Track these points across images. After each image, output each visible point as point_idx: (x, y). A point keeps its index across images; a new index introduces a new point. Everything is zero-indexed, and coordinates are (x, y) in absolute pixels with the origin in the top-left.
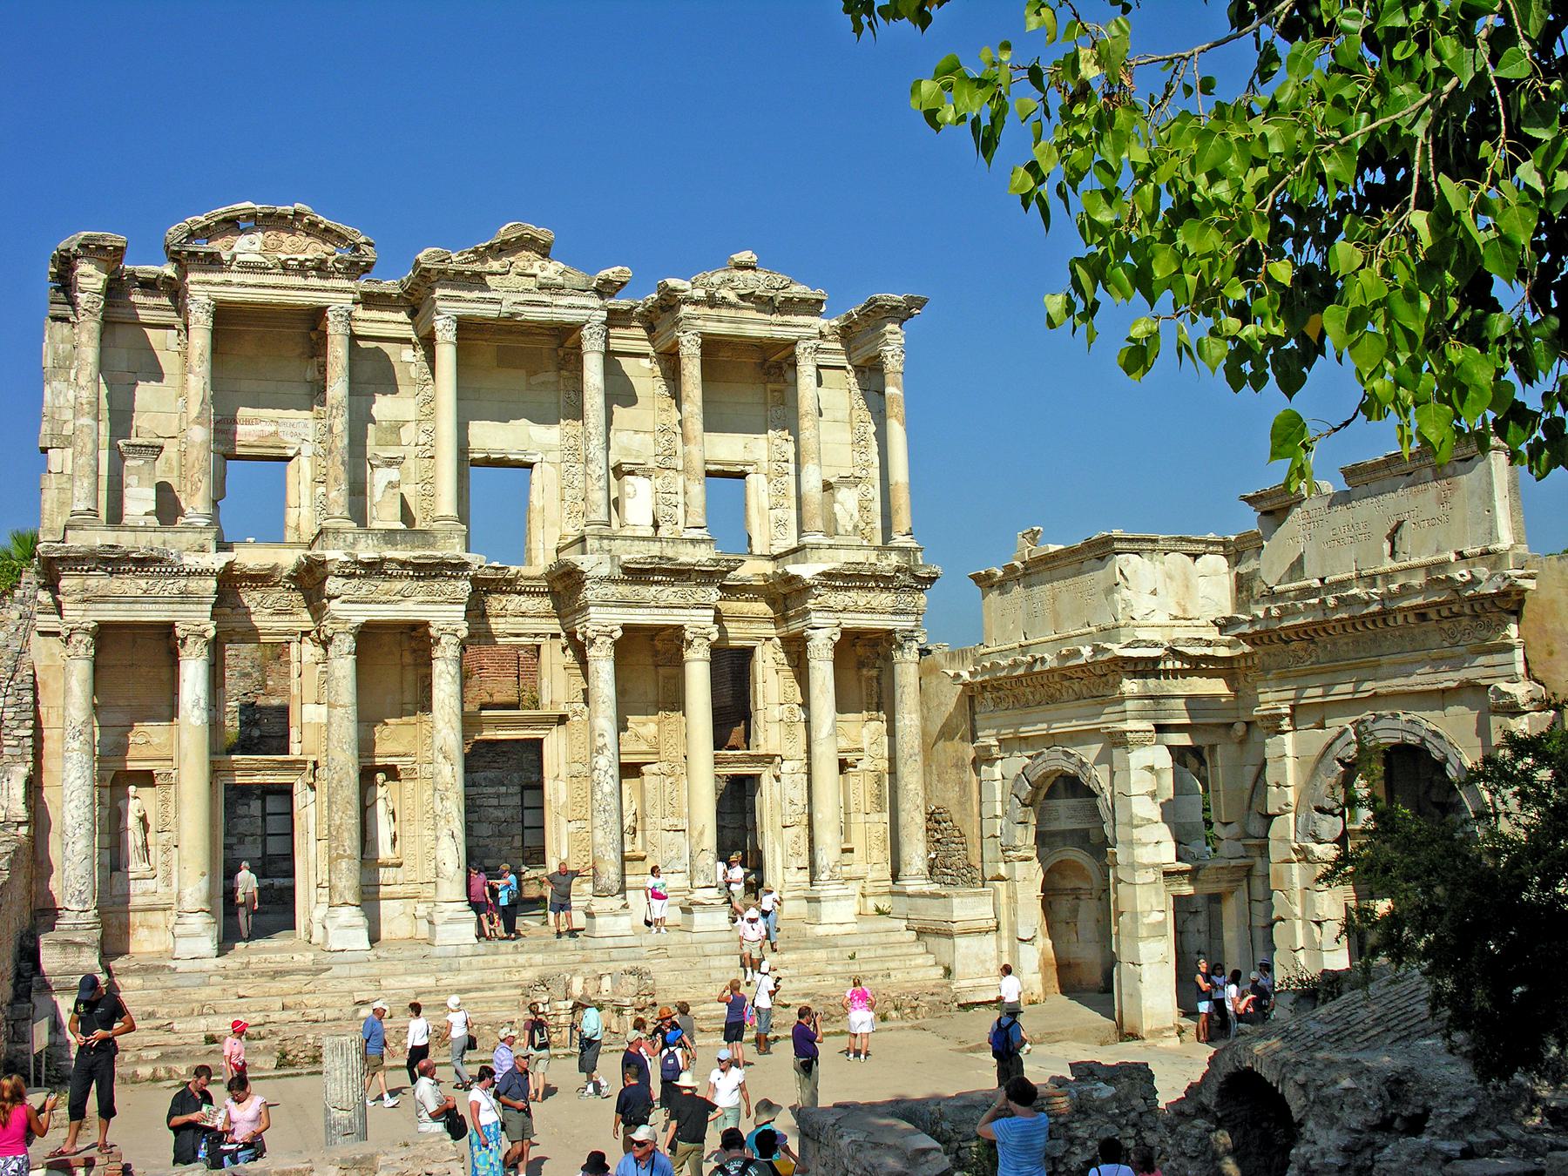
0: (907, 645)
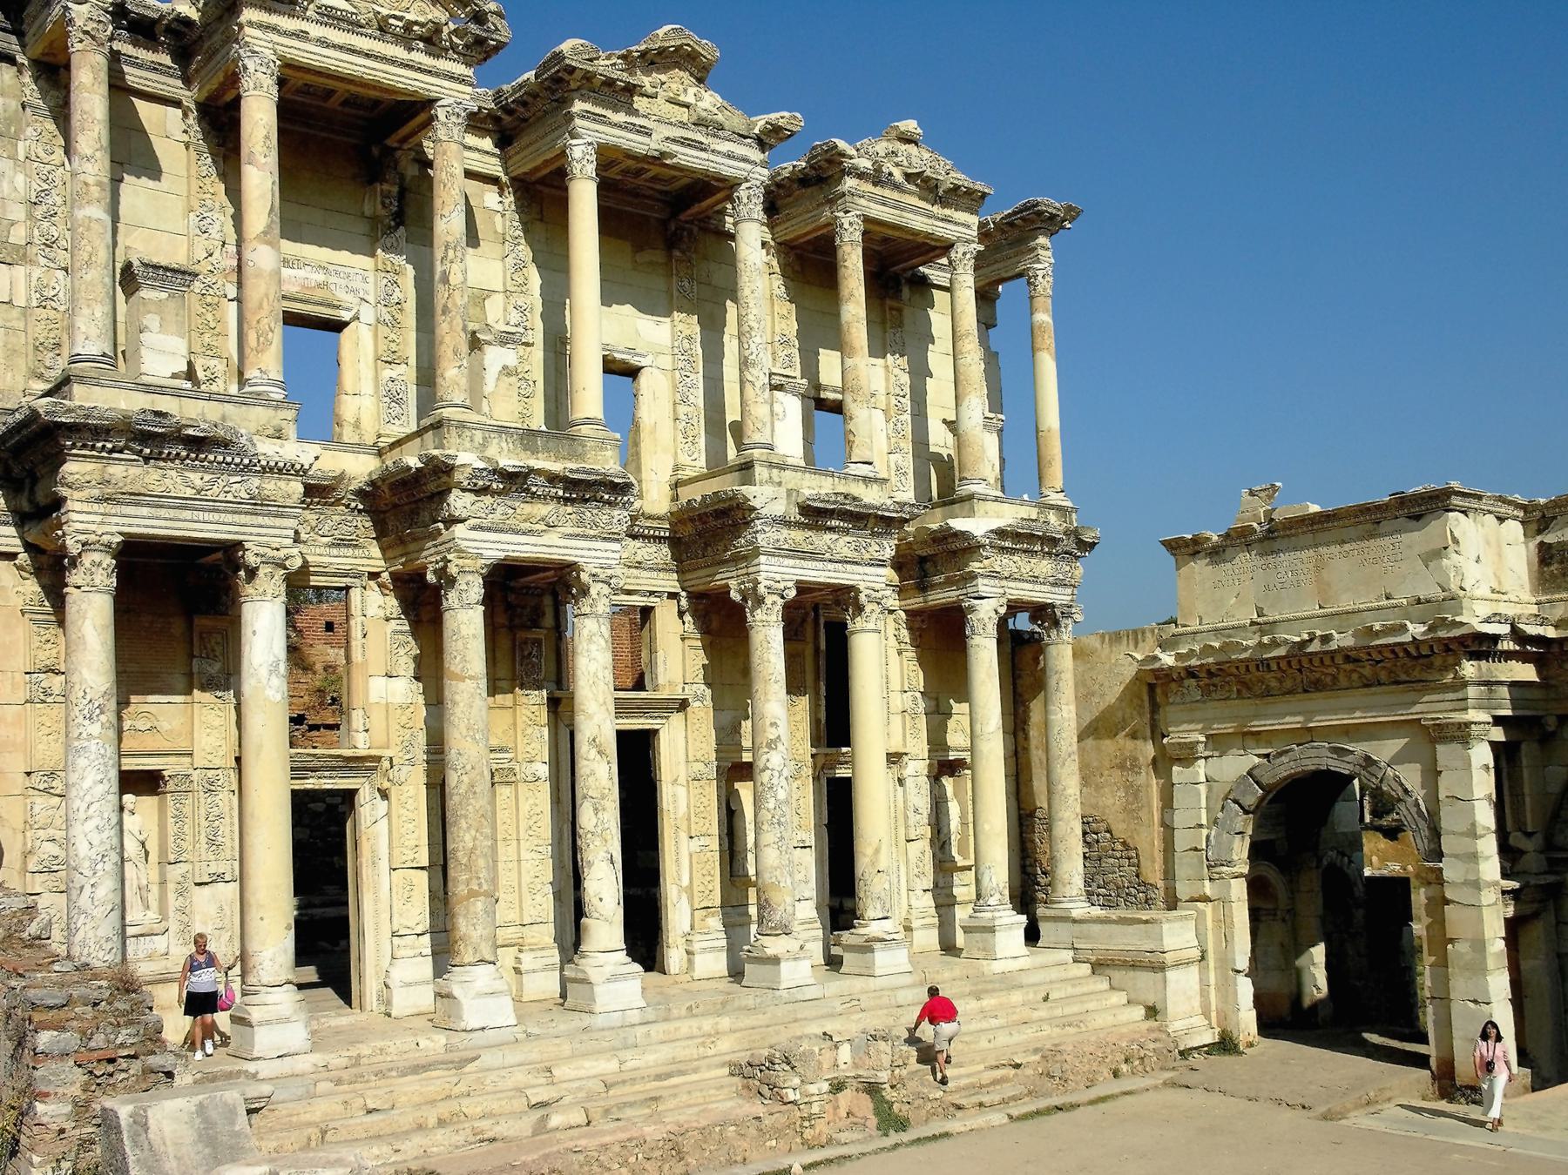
0: (1063, 622)
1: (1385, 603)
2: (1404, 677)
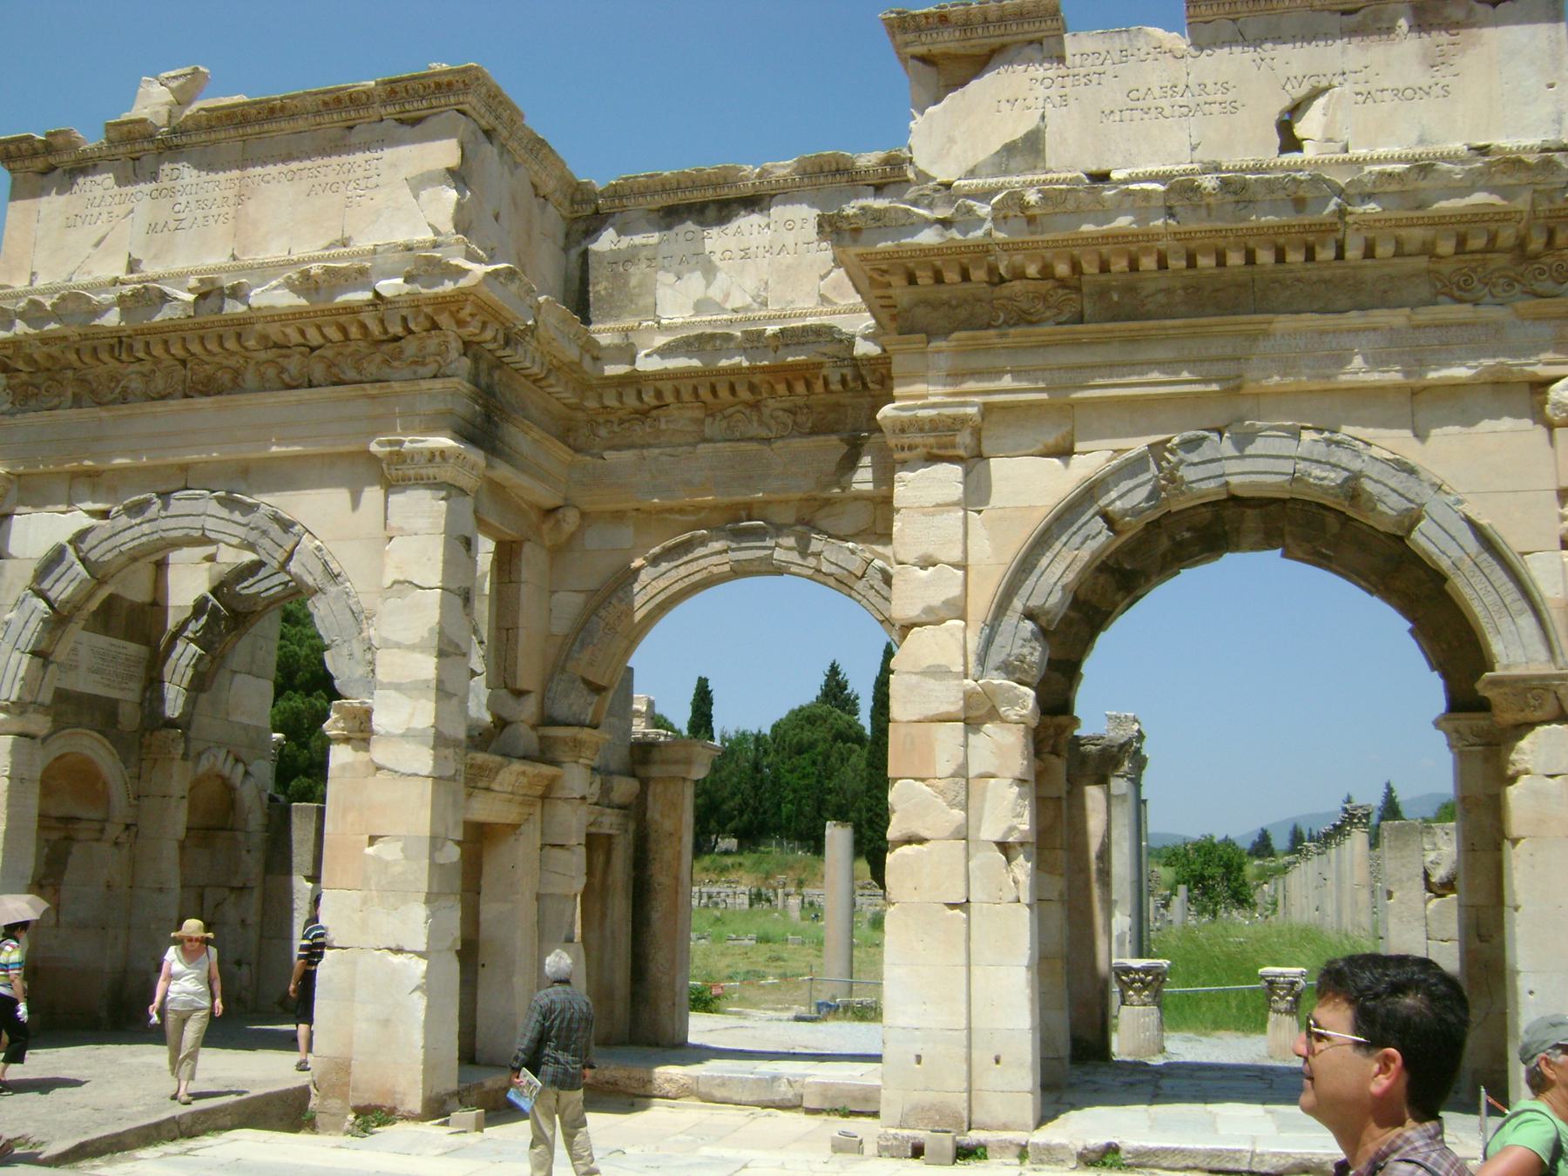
2: (352, 374)
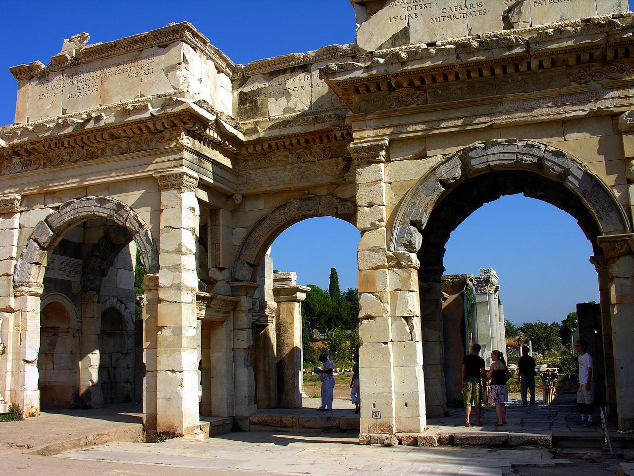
1: (139, 99)
